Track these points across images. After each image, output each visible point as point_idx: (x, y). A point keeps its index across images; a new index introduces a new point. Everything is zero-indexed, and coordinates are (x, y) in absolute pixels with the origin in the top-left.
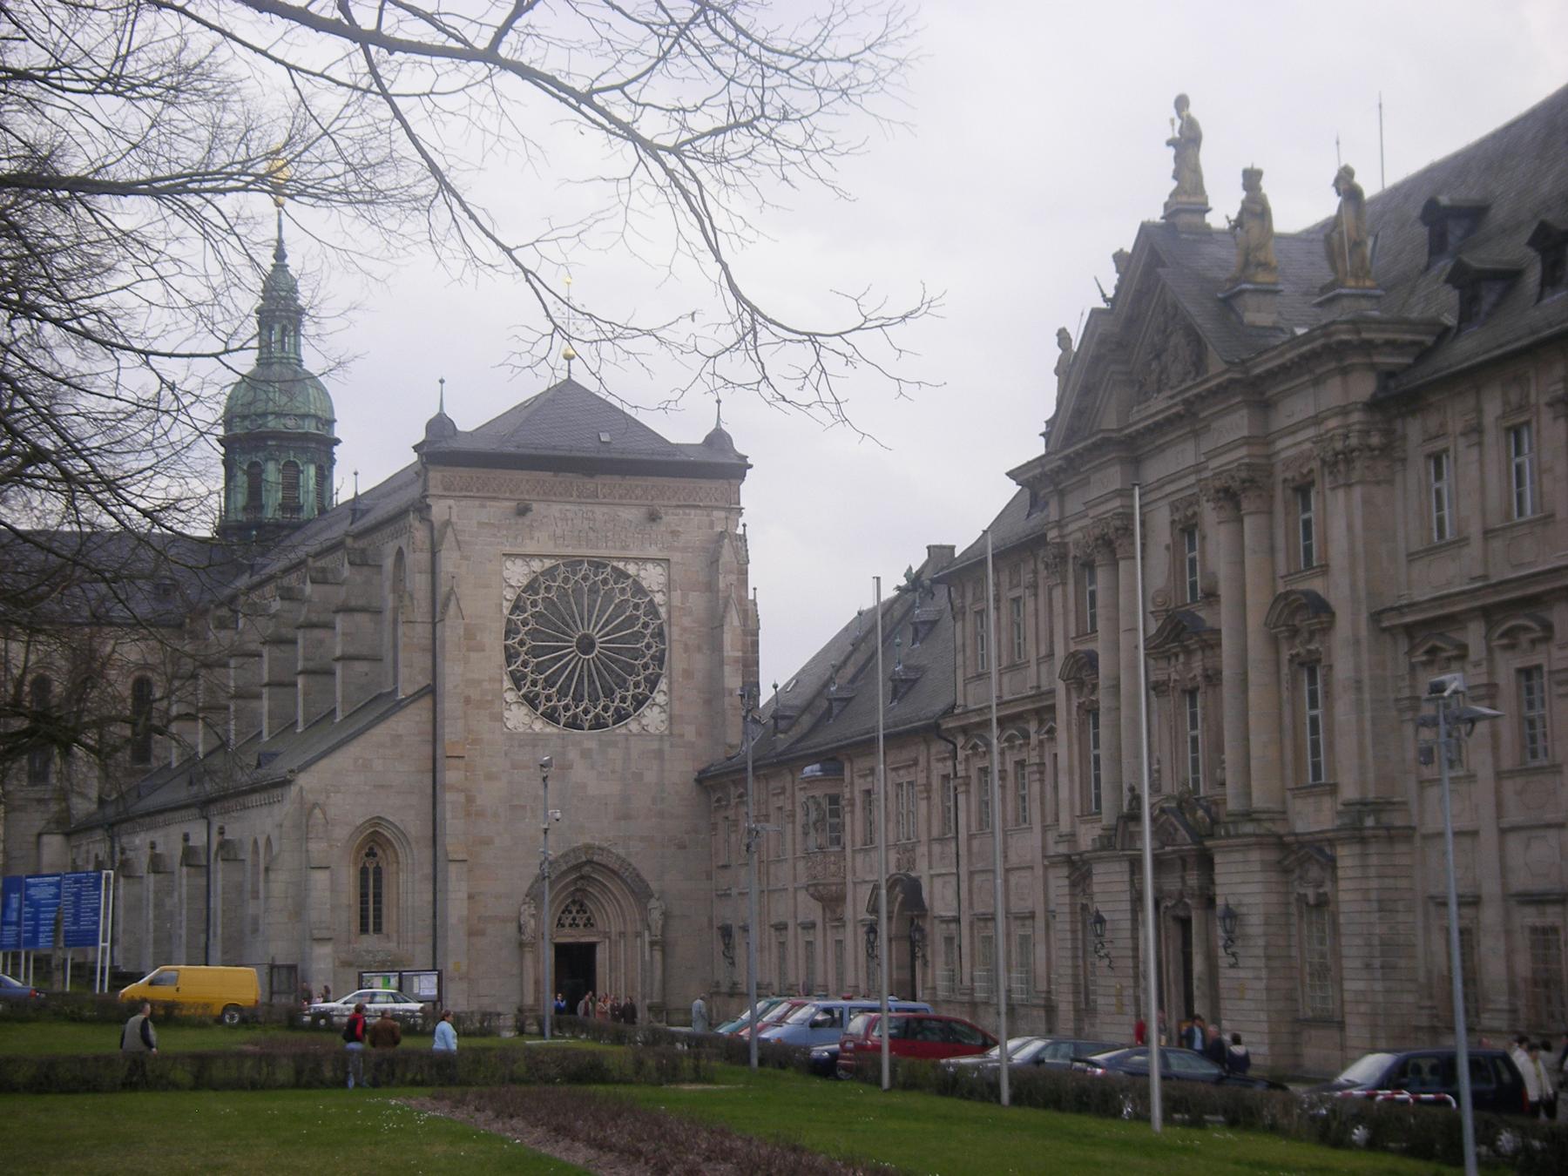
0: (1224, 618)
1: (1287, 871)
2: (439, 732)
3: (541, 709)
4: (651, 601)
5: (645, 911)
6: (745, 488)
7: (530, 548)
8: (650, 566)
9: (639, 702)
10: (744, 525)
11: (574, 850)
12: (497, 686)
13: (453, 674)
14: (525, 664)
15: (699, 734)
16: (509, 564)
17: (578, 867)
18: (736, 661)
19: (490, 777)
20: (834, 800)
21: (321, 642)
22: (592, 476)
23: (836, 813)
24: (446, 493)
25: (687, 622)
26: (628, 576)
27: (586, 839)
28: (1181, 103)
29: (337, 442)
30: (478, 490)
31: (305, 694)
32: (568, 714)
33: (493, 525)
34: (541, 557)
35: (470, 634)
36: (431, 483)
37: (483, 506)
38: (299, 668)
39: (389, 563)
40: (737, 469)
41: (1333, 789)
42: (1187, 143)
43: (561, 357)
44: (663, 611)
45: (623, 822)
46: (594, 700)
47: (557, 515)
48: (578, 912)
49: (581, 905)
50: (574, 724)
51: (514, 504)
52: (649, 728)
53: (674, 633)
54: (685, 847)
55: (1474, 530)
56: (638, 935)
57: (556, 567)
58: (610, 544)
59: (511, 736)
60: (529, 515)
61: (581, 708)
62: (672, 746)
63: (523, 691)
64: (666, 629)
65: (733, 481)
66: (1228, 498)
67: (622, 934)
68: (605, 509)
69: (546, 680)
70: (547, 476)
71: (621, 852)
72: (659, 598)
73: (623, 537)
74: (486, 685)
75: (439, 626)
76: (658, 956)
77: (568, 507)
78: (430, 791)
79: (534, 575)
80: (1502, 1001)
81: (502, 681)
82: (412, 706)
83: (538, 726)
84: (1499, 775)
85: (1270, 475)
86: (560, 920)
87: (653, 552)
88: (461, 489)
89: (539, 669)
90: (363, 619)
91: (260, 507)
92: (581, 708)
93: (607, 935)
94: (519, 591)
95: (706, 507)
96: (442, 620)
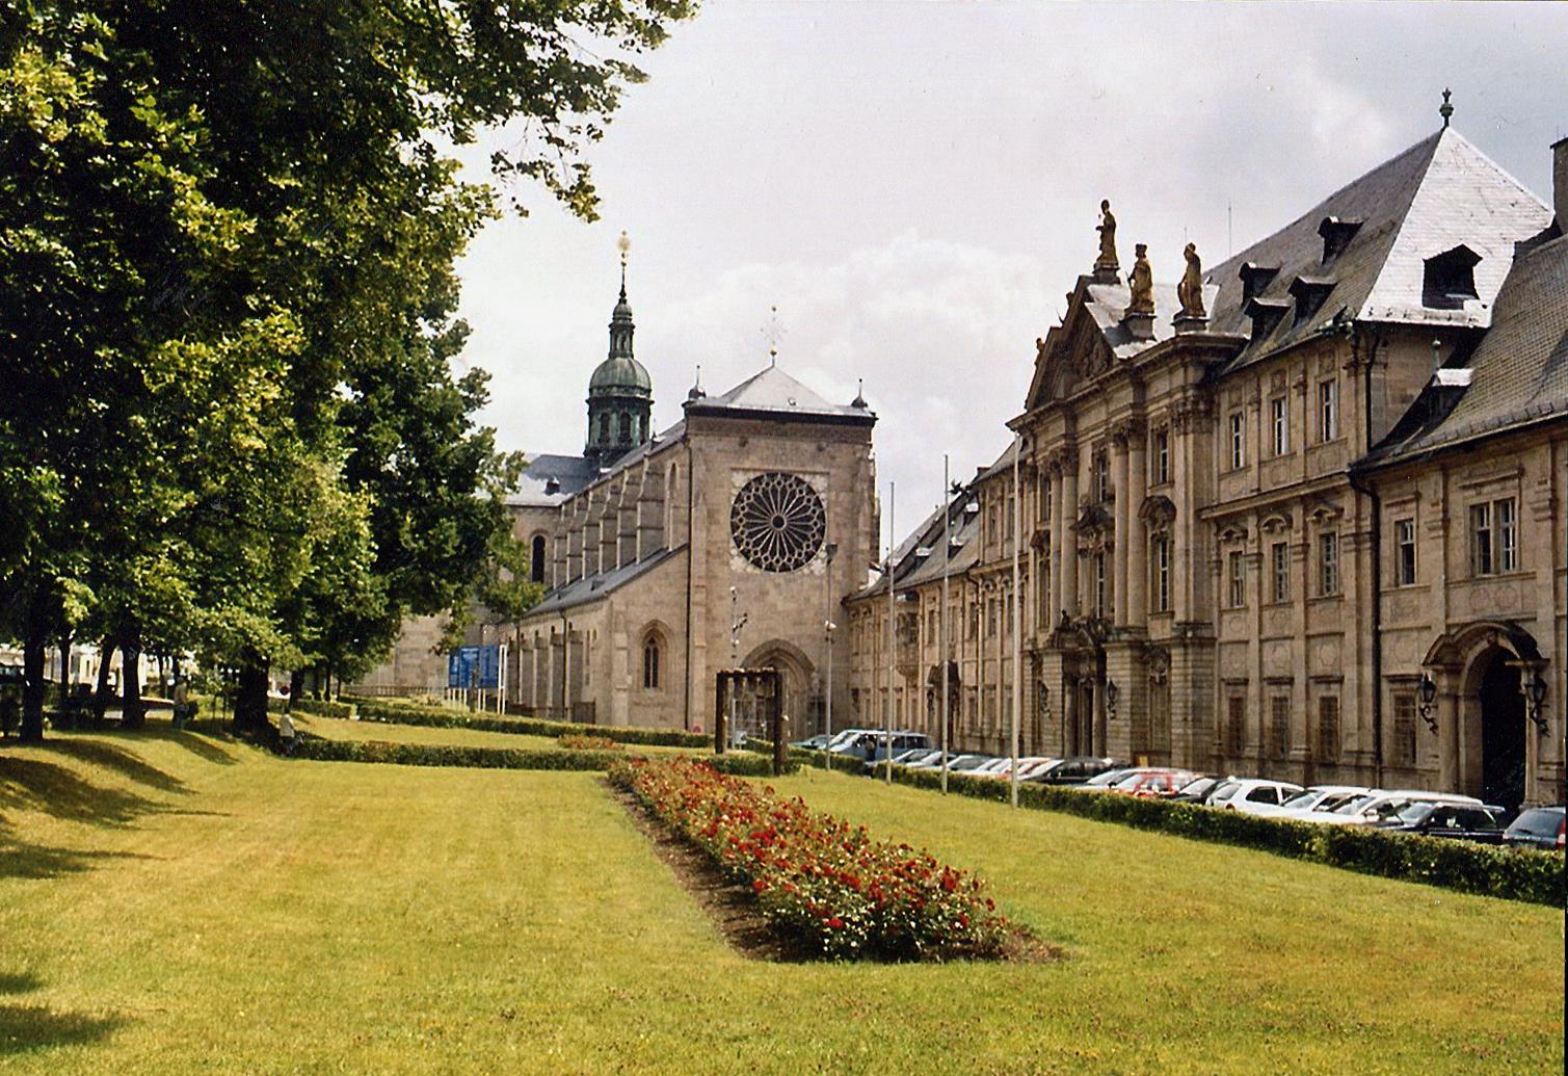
0: (1116, 511)
1: (1145, 663)
5: (809, 680)
6: (873, 431)
7: (747, 465)
8: (818, 477)
9: (809, 556)
12: (725, 545)
13: (699, 539)
14: (742, 533)
15: (844, 576)
16: (735, 474)
17: (772, 651)
18: (867, 533)
20: (913, 616)
23: (915, 624)
25: (838, 510)
26: (804, 483)
28: (1105, 205)
29: (653, 402)
31: (622, 548)
34: (755, 470)
35: (710, 514)
39: (668, 473)
40: (871, 421)
41: (1172, 614)
42: (1108, 229)
44: (824, 504)
46: (783, 554)
50: (770, 568)
55: (1254, 462)
57: (762, 477)
60: (747, 446)
66: (1121, 440)
71: (796, 643)
74: (720, 545)
80: (1256, 741)
83: (750, 569)
84: (1261, 608)
85: (1145, 427)
87: (819, 468)
89: (751, 535)
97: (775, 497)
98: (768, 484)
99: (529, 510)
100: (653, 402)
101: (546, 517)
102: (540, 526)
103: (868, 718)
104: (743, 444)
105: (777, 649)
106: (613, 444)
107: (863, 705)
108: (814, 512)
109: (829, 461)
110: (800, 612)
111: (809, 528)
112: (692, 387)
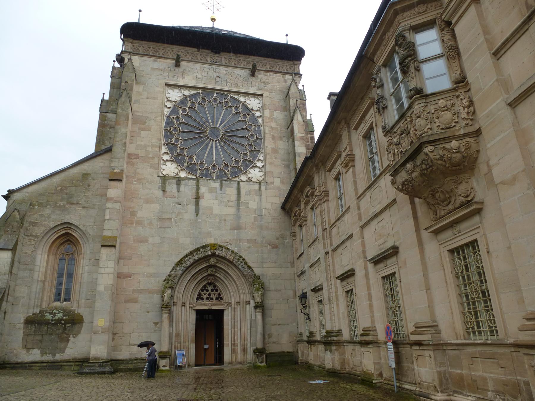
3: (186, 164)
7: (182, 82)
8: (252, 99)
10: (303, 86)
11: (203, 247)
12: (157, 149)
15: (282, 182)
16: (170, 91)
17: (206, 258)
18: (302, 138)
19: (148, 201)
22: (218, 53)
25: (273, 125)
26: (240, 102)
27: (210, 241)
37: (156, 61)
44: (260, 120)
45: (236, 231)
48: (212, 290)
49: (215, 286)
51: (174, 62)
52: (253, 180)
54: (276, 247)
56: (248, 303)
62: (266, 189)
64: (262, 128)
65: (295, 62)
67: (239, 303)
68: (226, 69)
72: (257, 114)
74: (149, 149)
76: (259, 316)
79: (183, 97)
81: (160, 148)
86: (200, 294)
93: (229, 304)
103: (322, 324)
104: (177, 65)
105: (214, 255)
107: (314, 309)
110: (238, 217)
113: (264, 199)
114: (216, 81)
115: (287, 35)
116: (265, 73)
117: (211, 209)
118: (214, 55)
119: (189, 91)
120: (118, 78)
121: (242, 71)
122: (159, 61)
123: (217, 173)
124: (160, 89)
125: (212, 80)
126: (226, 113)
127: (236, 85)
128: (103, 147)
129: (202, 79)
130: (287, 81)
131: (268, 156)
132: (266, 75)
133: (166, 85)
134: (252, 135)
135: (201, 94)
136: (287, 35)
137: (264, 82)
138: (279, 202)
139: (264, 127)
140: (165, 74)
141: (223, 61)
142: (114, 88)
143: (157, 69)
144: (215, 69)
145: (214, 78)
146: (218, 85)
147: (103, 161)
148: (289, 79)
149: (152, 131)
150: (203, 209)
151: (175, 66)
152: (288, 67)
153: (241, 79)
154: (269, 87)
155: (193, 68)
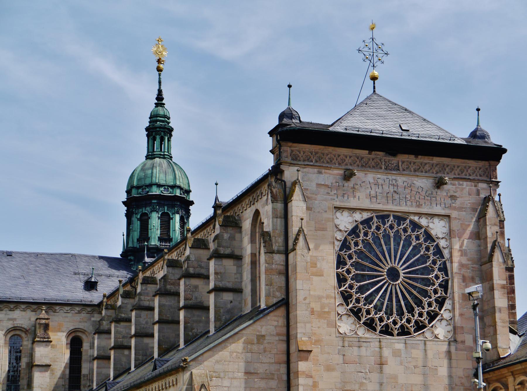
2: (292, 332)
3: (363, 320)
4: (437, 246)
7: (353, 203)
8: (436, 220)
9: (432, 316)
10: (499, 195)
12: (333, 301)
14: (351, 287)
16: (338, 214)
18: (503, 287)
19: (329, 369)
21: (196, 287)
22: (394, 155)
24: (293, 162)
29: (192, 203)
30: (316, 161)
32: (382, 324)
33: (327, 186)
36: (284, 155)
37: (320, 173)
38: (181, 306)
43: (368, 79)
44: (446, 253)
47: (372, 181)
50: (387, 331)
51: (342, 172)
52: (439, 336)
53: (455, 267)
57: (371, 219)
58: (409, 203)
59: (343, 336)
60: (353, 180)
61: (391, 320)
62: (456, 349)
63: (351, 306)
64: (448, 265)
65: (492, 163)
68: (404, 179)
69: (366, 299)
70: (364, 153)
72: (443, 243)
73: (417, 199)
74: (325, 301)
75: (291, 256)
77: (379, 176)
78: (285, 377)
82: (271, 314)
87: (438, 210)
88: (304, 161)
89: (361, 290)
90: (229, 264)
91: (148, 239)
92: (391, 320)
94: (346, 234)
95: (474, 180)
96: (294, 249)
97: (387, 243)
98: (378, 228)
99: (67, 308)
100: (192, 203)
101: (84, 315)
102: (81, 326)
106: (154, 242)
108: (434, 262)
109: (449, 201)
111: (428, 282)
112: (283, 108)
113: (454, 363)
114: (394, 198)
115: (478, 110)
116: (452, 182)
117: (395, 377)
118: (389, 158)
119: (360, 213)
120: (280, 202)
121: (424, 180)
122: (324, 172)
123: (398, 330)
124: (329, 215)
125: (388, 198)
126: (405, 243)
127: (418, 203)
128: (275, 301)
129: (376, 197)
130: (481, 191)
131: (457, 306)
132: (453, 185)
133: (335, 207)
134: (436, 275)
135: (375, 219)
136: (478, 110)
137: (451, 196)
138: (471, 367)
139: (452, 262)
140: (333, 193)
141: (400, 165)
142: (277, 218)
143: (323, 185)
144: (391, 180)
145: (391, 193)
146: (396, 205)
147: (276, 318)
148: (483, 189)
149: (325, 275)
150: (387, 378)
151: (344, 180)
152: (482, 169)
153: (423, 193)
154: (458, 203)
155: (364, 180)
